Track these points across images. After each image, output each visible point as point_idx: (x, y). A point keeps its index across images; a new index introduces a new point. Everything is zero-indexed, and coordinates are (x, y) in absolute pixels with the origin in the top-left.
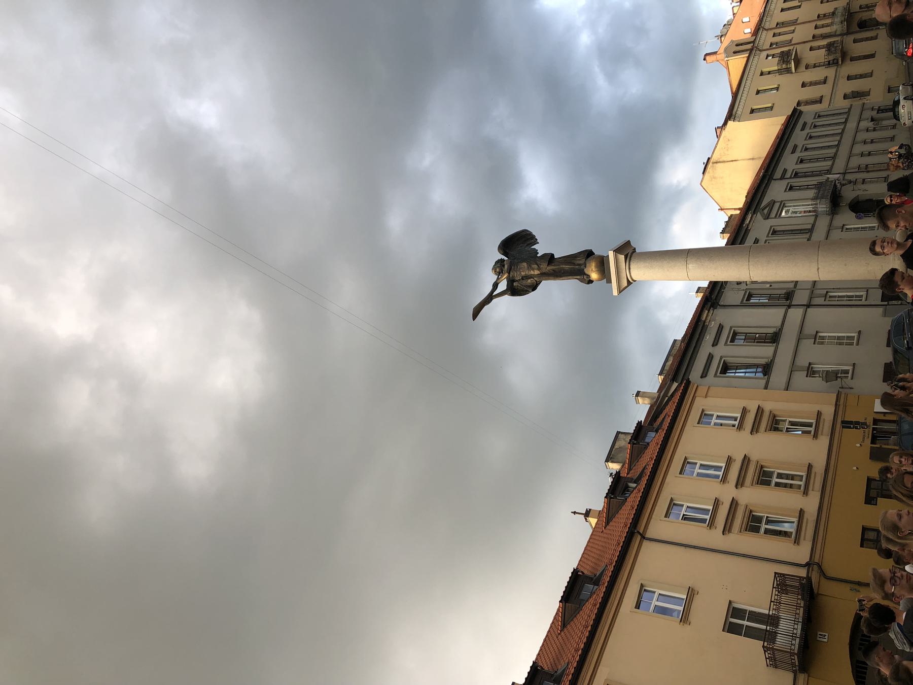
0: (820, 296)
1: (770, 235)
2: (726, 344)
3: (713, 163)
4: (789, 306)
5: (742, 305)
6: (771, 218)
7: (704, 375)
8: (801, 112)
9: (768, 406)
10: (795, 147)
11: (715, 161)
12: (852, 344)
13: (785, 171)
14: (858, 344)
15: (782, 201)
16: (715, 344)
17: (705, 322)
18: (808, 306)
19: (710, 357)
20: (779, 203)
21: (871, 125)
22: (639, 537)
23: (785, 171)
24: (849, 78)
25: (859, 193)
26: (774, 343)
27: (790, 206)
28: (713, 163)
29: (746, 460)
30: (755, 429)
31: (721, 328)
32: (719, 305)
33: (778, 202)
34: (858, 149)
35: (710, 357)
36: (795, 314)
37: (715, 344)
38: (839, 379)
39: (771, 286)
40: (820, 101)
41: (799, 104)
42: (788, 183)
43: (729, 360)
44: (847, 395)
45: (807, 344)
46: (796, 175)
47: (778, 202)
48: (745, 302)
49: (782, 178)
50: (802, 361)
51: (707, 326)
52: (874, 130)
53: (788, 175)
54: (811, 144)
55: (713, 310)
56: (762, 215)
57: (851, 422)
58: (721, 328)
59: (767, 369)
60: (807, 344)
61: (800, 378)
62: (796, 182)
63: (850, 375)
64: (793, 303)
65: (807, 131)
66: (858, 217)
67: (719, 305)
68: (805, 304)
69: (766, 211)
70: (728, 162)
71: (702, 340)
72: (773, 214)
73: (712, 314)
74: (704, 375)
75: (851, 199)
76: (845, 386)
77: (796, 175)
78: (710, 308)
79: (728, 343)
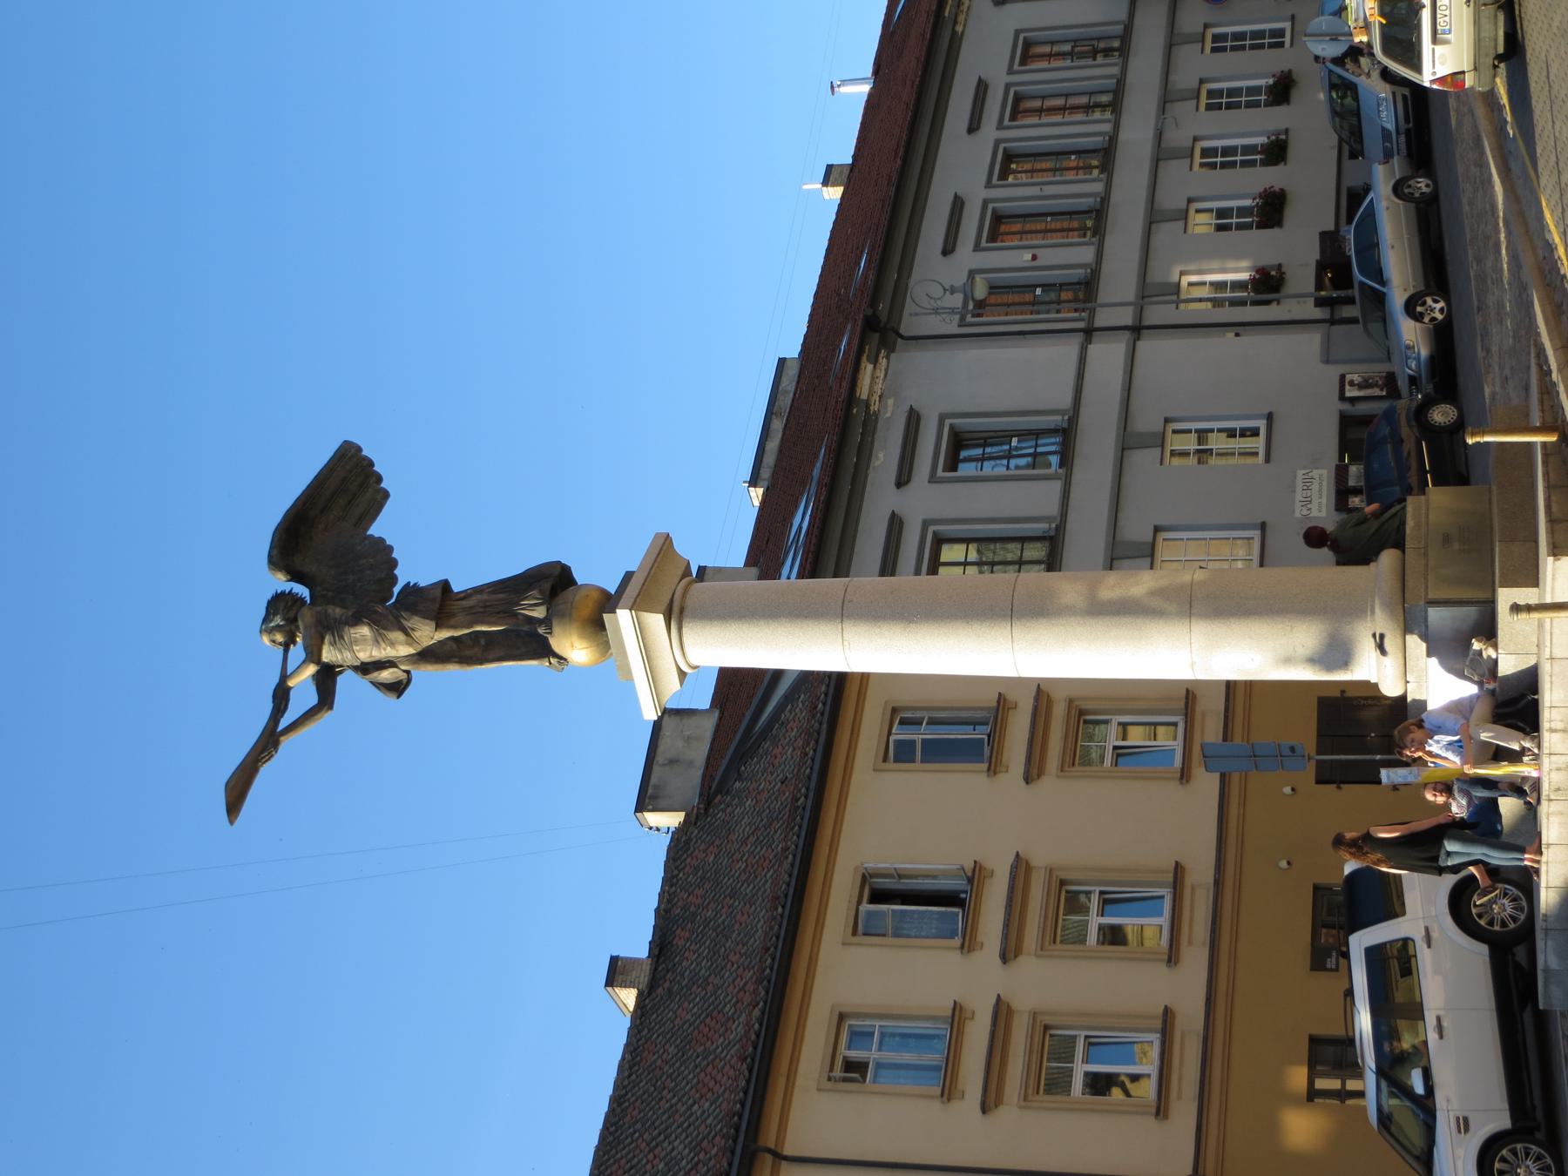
2: (933, 479)
4: (1089, 333)
16: (902, 481)
17: (867, 404)
18: (1137, 330)
19: (896, 524)
22: (769, 1158)
31: (914, 420)
32: (902, 337)
35: (896, 524)
36: (1108, 356)
37: (902, 481)
39: (1034, 258)
51: (877, 419)
55: (888, 358)
58: (914, 420)
67: (902, 337)
71: (867, 469)
73: (886, 370)
78: (878, 353)
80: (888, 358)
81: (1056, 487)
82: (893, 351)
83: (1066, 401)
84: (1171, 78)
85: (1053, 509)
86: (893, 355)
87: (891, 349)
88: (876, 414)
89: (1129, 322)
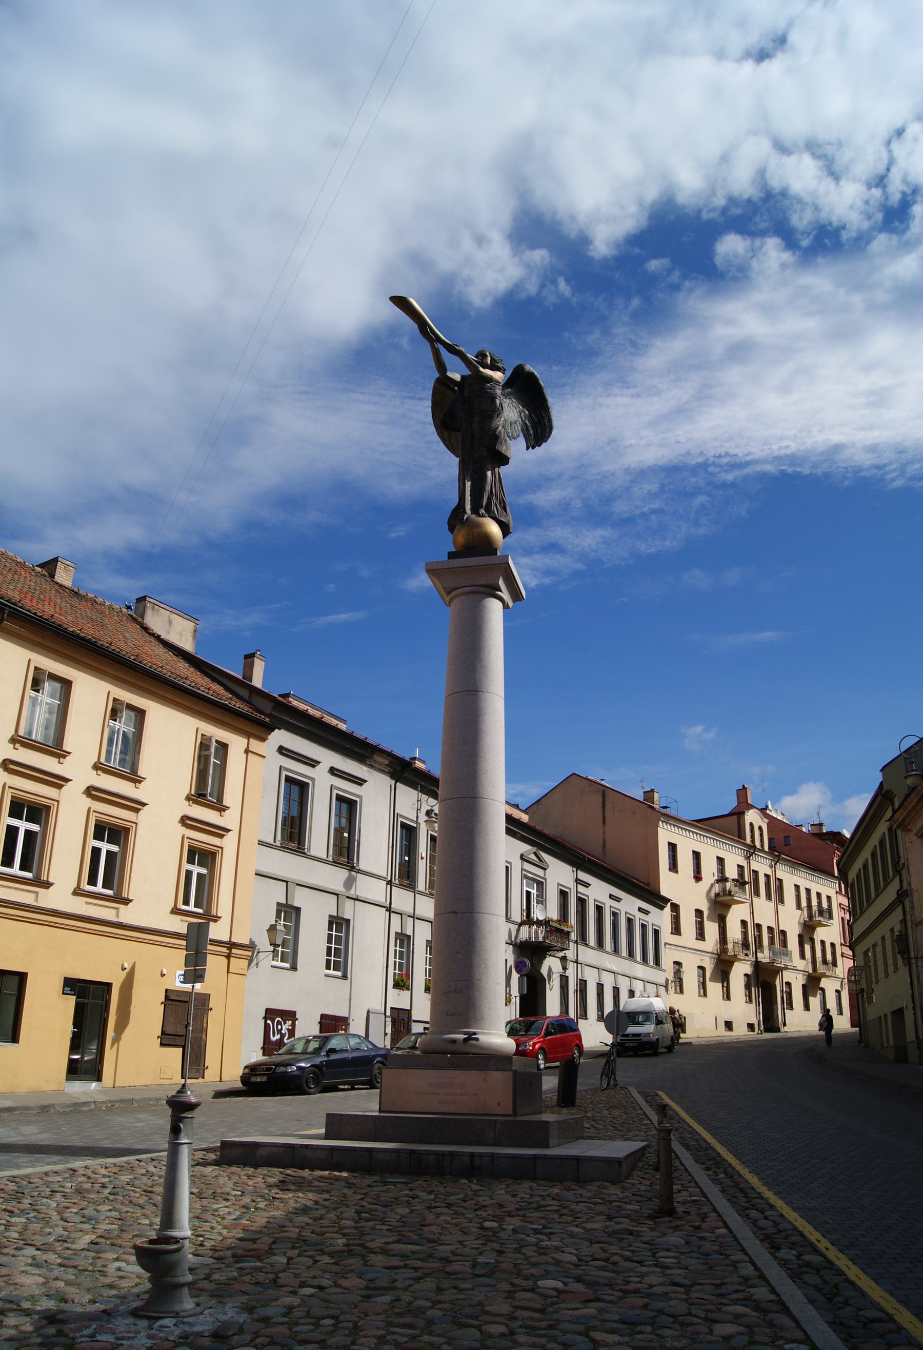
4: (390, 883)
5: (395, 816)
6: (522, 864)
8: (662, 908)
9: (229, 843)
10: (618, 900)
13: (587, 885)
16: (333, 771)
19: (312, 763)
20: (543, 876)
23: (587, 885)
29: (136, 806)
30: (185, 821)
31: (360, 782)
33: (545, 875)
35: (312, 763)
37: (333, 771)
42: (570, 889)
47: (545, 875)
48: (400, 819)
49: (578, 881)
53: (581, 889)
58: (360, 782)
60: (329, 906)
65: (639, 915)
69: (533, 857)
72: (527, 866)
85: (313, 853)
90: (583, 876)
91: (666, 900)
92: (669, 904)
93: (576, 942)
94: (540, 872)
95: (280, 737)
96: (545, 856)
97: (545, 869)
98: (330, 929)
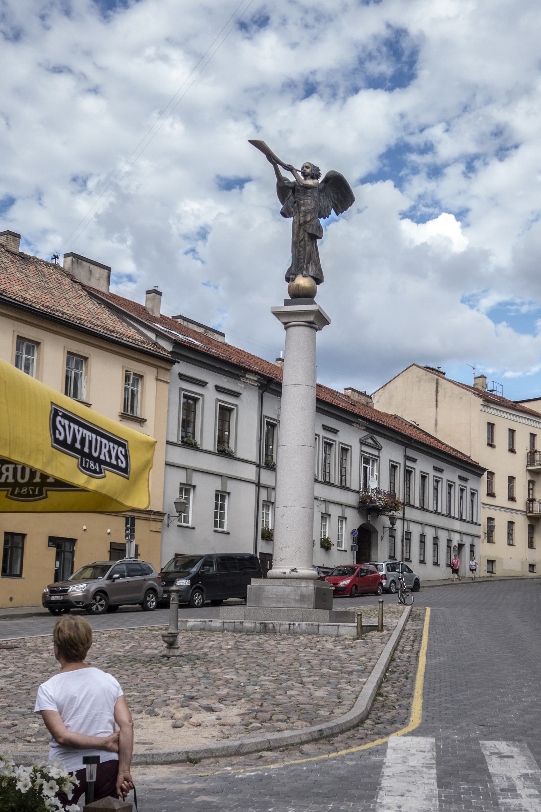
0: (269, 496)
1: (341, 445)
2: (218, 400)
3: (437, 380)
4: (259, 466)
5: (261, 416)
6: (360, 448)
7: (182, 377)
8: (480, 476)
10: (441, 471)
11: (439, 382)
12: (215, 526)
14: (215, 531)
15: (379, 457)
17: (244, 377)
19: (203, 384)
21: (455, 543)
23: (414, 460)
24: (511, 524)
25: (380, 534)
26: (218, 450)
27: (373, 466)
28: (437, 380)
31: (236, 395)
32: (263, 393)
33: (379, 454)
34: (430, 533)
35: (203, 384)
36: (250, 472)
37: (218, 389)
38: (177, 514)
40: (491, 494)
41: (491, 474)
42: (399, 464)
43: (199, 405)
44: (161, 521)
45: (217, 484)
46: (408, 472)
48: (266, 419)
49: (407, 458)
50: (196, 479)
51: (237, 379)
52: (449, 547)
53: (409, 463)
54: (443, 488)
55: (257, 386)
56: (366, 437)
57: (133, 525)
58: (236, 395)
59: (327, 483)
60: (217, 484)
61: (180, 477)
62: (400, 473)
63: (182, 524)
64: (262, 470)
65: (458, 482)
66: (353, 532)
67: (263, 393)
68: (261, 482)
69: (370, 441)
70: (437, 396)
71: (222, 374)
72: (364, 448)
73: (253, 385)
74: (182, 377)
75: (375, 527)
76: (172, 519)
77: (408, 472)
78: (260, 383)
79: (219, 403)
80: (257, 386)
81: (211, 449)
82: (259, 389)
83: (239, 455)
84: (332, 505)
85: (205, 447)
86: (257, 388)
87: (260, 388)
88: (239, 380)
89: (262, 482)
90: (411, 453)
91: (484, 470)
92: (486, 473)
93: (403, 504)
94: (375, 452)
95: (180, 368)
96: (378, 439)
97: (379, 450)
98: (217, 499)
